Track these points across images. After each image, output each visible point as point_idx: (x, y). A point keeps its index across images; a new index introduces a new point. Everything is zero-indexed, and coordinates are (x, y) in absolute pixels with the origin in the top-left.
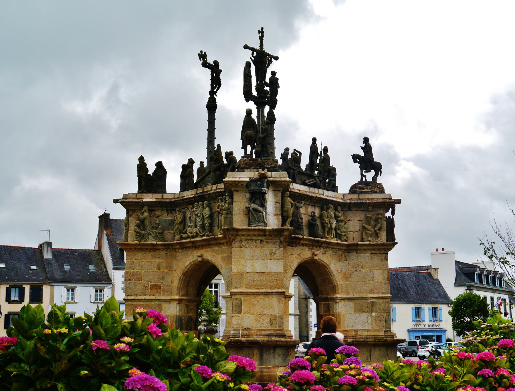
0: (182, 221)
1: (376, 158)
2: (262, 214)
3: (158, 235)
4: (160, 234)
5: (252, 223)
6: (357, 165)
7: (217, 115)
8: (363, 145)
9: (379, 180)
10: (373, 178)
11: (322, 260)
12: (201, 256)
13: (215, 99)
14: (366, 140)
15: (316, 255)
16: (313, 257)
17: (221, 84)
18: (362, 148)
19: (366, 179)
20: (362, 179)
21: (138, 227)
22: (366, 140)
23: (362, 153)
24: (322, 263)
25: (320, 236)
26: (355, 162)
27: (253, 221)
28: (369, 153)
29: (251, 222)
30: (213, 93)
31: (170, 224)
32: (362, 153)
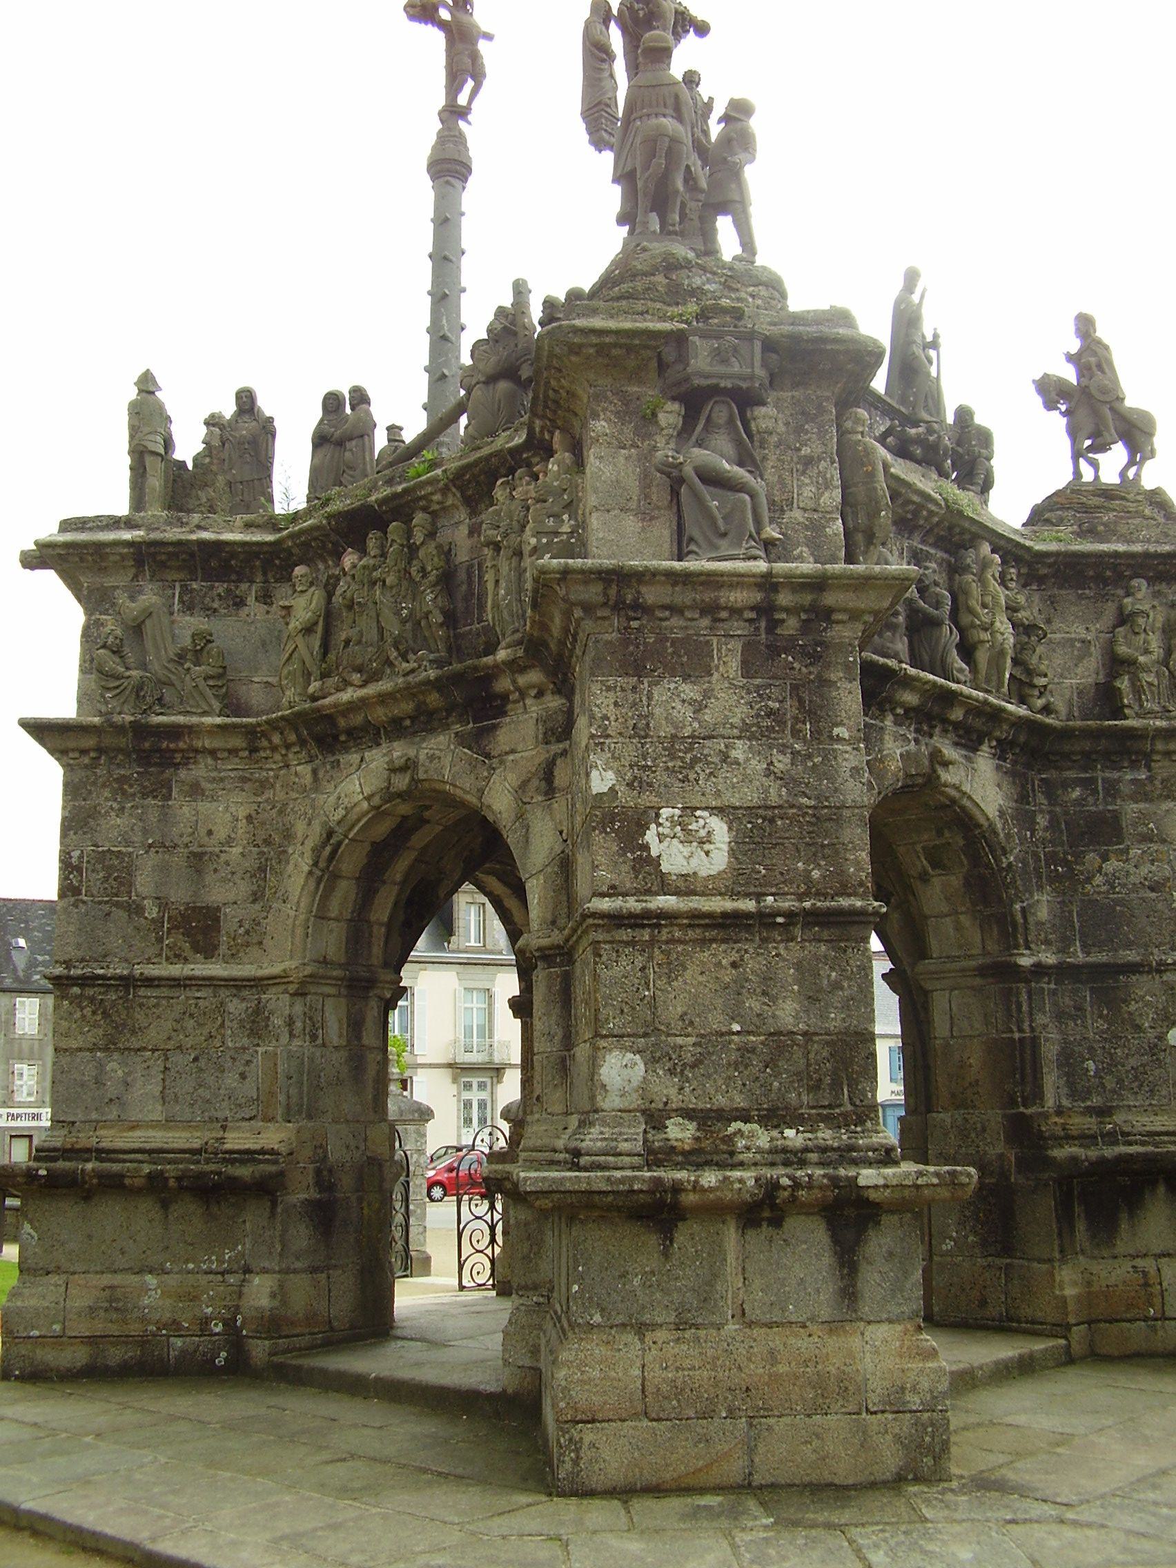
0: (316, 623)
1: (1134, 398)
2: (747, 497)
3: (202, 683)
4: (211, 683)
5: (693, 547)
6: (1057, 422)
7: (472, 197)
8: (1074, 346)
9: (1151, 477)
10: (1123, 474)
11: (965, 793)
12: (409, 766)
13: (460, 139)
14: (1085, 325)
15: (946, 764)
16: (935, 771)
17: (484, 76)
18: (1070, 358)
19: (1097, 477)
20: (1077, 473)
21: (114, 652)
22: (1085, 325)
23: (1069, 374)
24: (963, 808)
25: (962, 678)
26: (1050, 405)
27: (696, 533)
28: (1105, 366)
29: (691, 539)
30: (453, 113)
31: (264, 644)
32: (1069, 374)
